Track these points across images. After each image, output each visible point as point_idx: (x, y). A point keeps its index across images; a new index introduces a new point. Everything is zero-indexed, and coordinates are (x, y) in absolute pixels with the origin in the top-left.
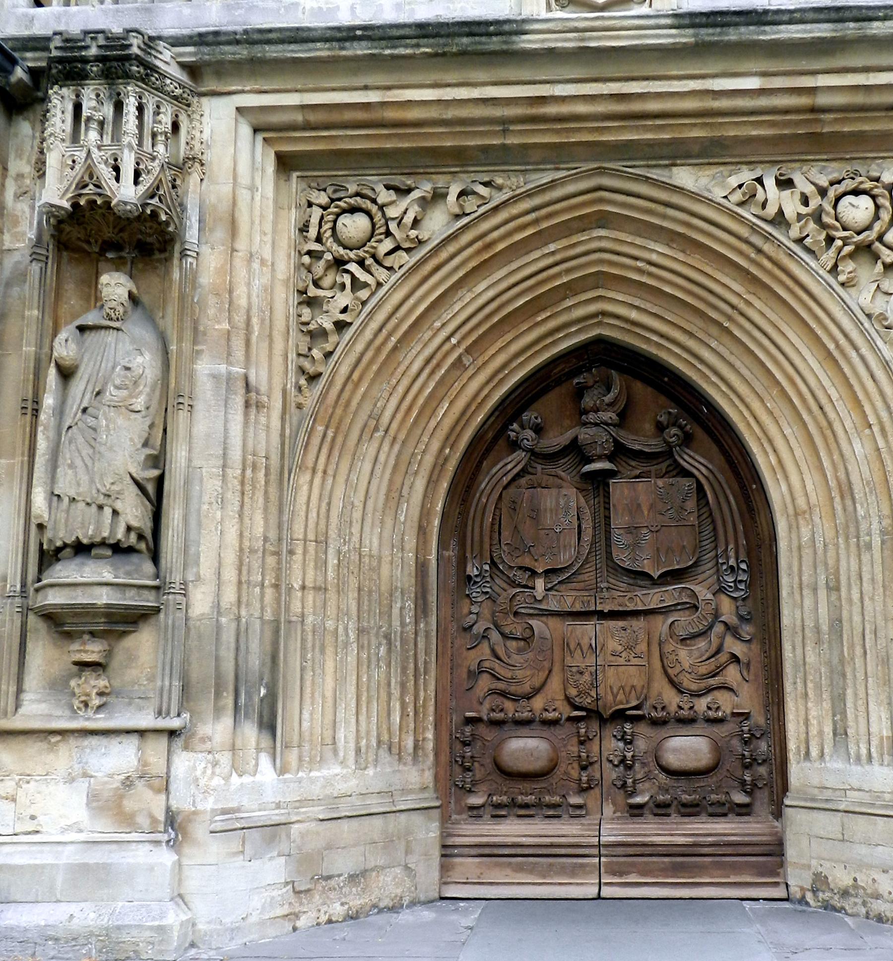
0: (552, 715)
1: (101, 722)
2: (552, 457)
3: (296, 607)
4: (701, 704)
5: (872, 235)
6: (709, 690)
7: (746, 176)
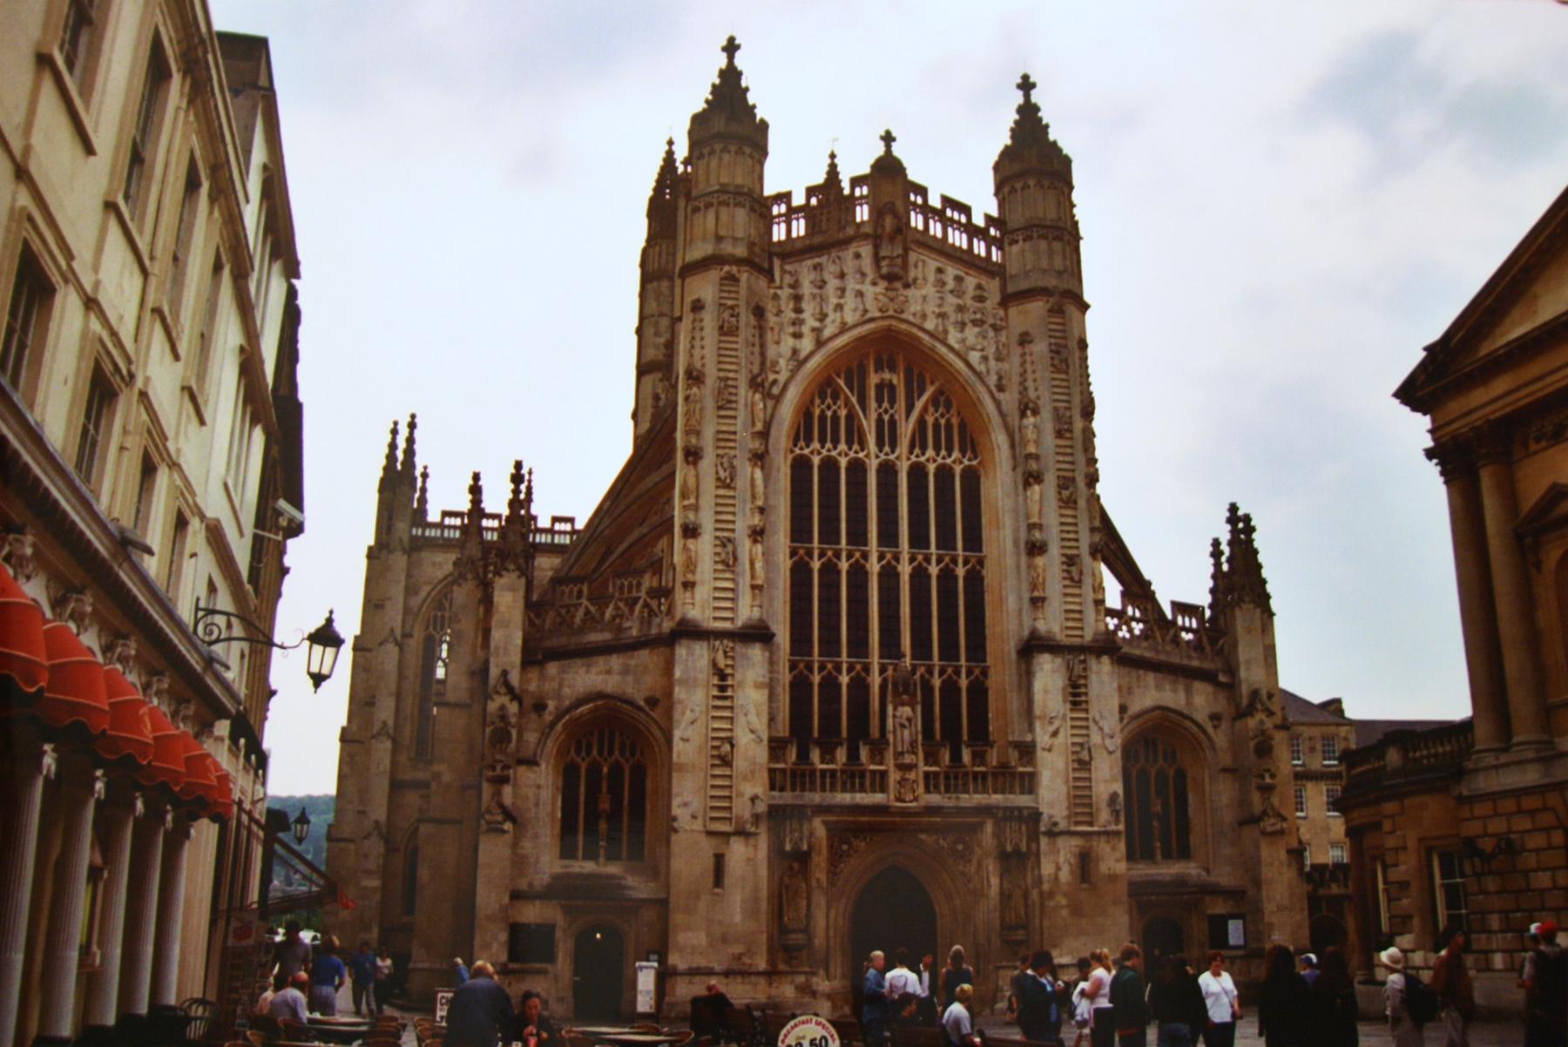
7: (934, 837)
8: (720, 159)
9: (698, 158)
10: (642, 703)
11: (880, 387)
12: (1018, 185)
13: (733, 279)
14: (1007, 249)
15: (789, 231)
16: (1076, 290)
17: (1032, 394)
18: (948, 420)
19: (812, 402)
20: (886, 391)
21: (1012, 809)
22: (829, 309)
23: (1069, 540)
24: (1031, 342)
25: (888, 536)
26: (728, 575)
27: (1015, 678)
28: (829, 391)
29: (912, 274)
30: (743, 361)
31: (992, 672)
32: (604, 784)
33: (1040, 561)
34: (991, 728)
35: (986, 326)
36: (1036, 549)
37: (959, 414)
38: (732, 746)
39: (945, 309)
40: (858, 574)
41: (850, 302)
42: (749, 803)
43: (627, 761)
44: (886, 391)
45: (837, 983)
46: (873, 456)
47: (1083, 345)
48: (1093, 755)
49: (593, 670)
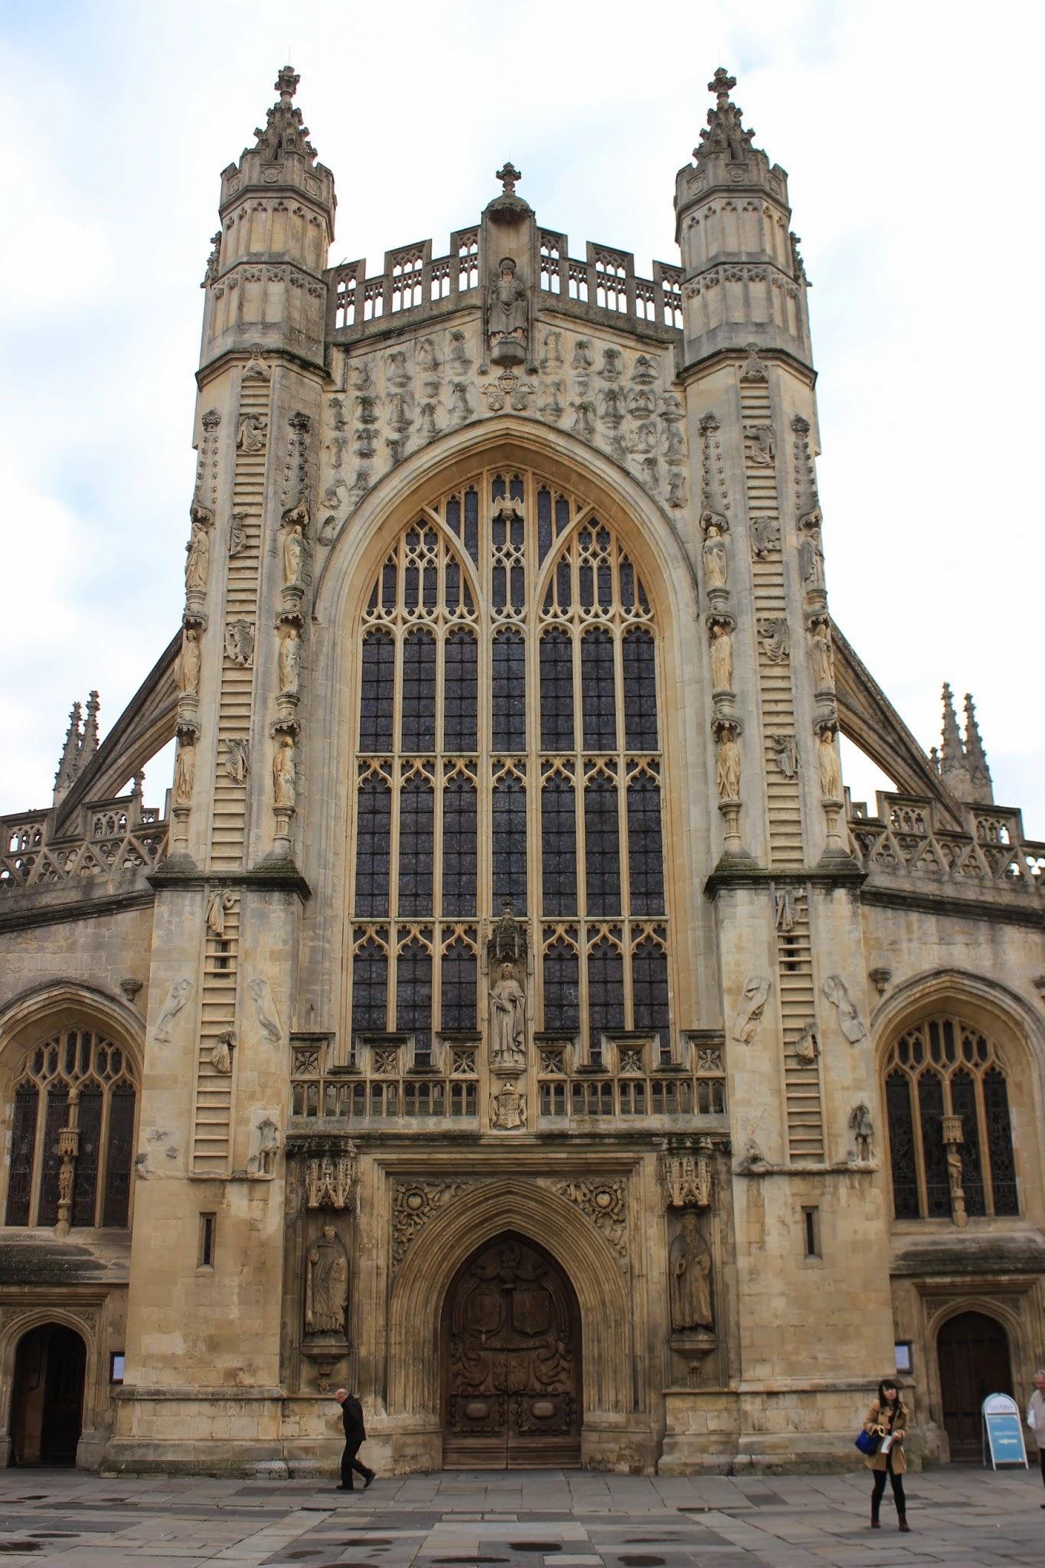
0: (488, 1393)
1: (330, 1395)
2: (489, 1281)
3: (393, 1351)
4: (550, 1388)
5: (609, 1209)
6: (553, 1382)
7: (564, 1184)
8: (251, 221)
9: (229, 227)
10: (117, 991)
11: (499, 520)
12: (699, 213)
13: (261, 377)
14: (684, 305)
15: (359, 312)
16: (791, 349)
17: (720, 503)
18: (604, 560)
19: (396, 551)
20: (508, 524)
21: (681, 1136)
22: (414, 414)
23: (778, 713)
24: (716, 428)
25: (509, 734)
26: (238, 795)
27: (700, 933)
28: (422, 533)
29: (540, 353)
30: (271, 489)
31: (670, 929)
32: (73, 1114)
33: (732, 749)
34: (671, 1016)
35: (654, 417)
36: (725, 731)
37: (620, 550)
38: (231, 1047)
39: (590, 397)
40: (462, 789)
41: (447, 397)
42: (258, 1132)
43: (108, 1078)
44: (508, 524)
45: (407, 1418)
46: (484, 618)
47: (803, 427)
48: (820, 1048)
49: (49, 945)
